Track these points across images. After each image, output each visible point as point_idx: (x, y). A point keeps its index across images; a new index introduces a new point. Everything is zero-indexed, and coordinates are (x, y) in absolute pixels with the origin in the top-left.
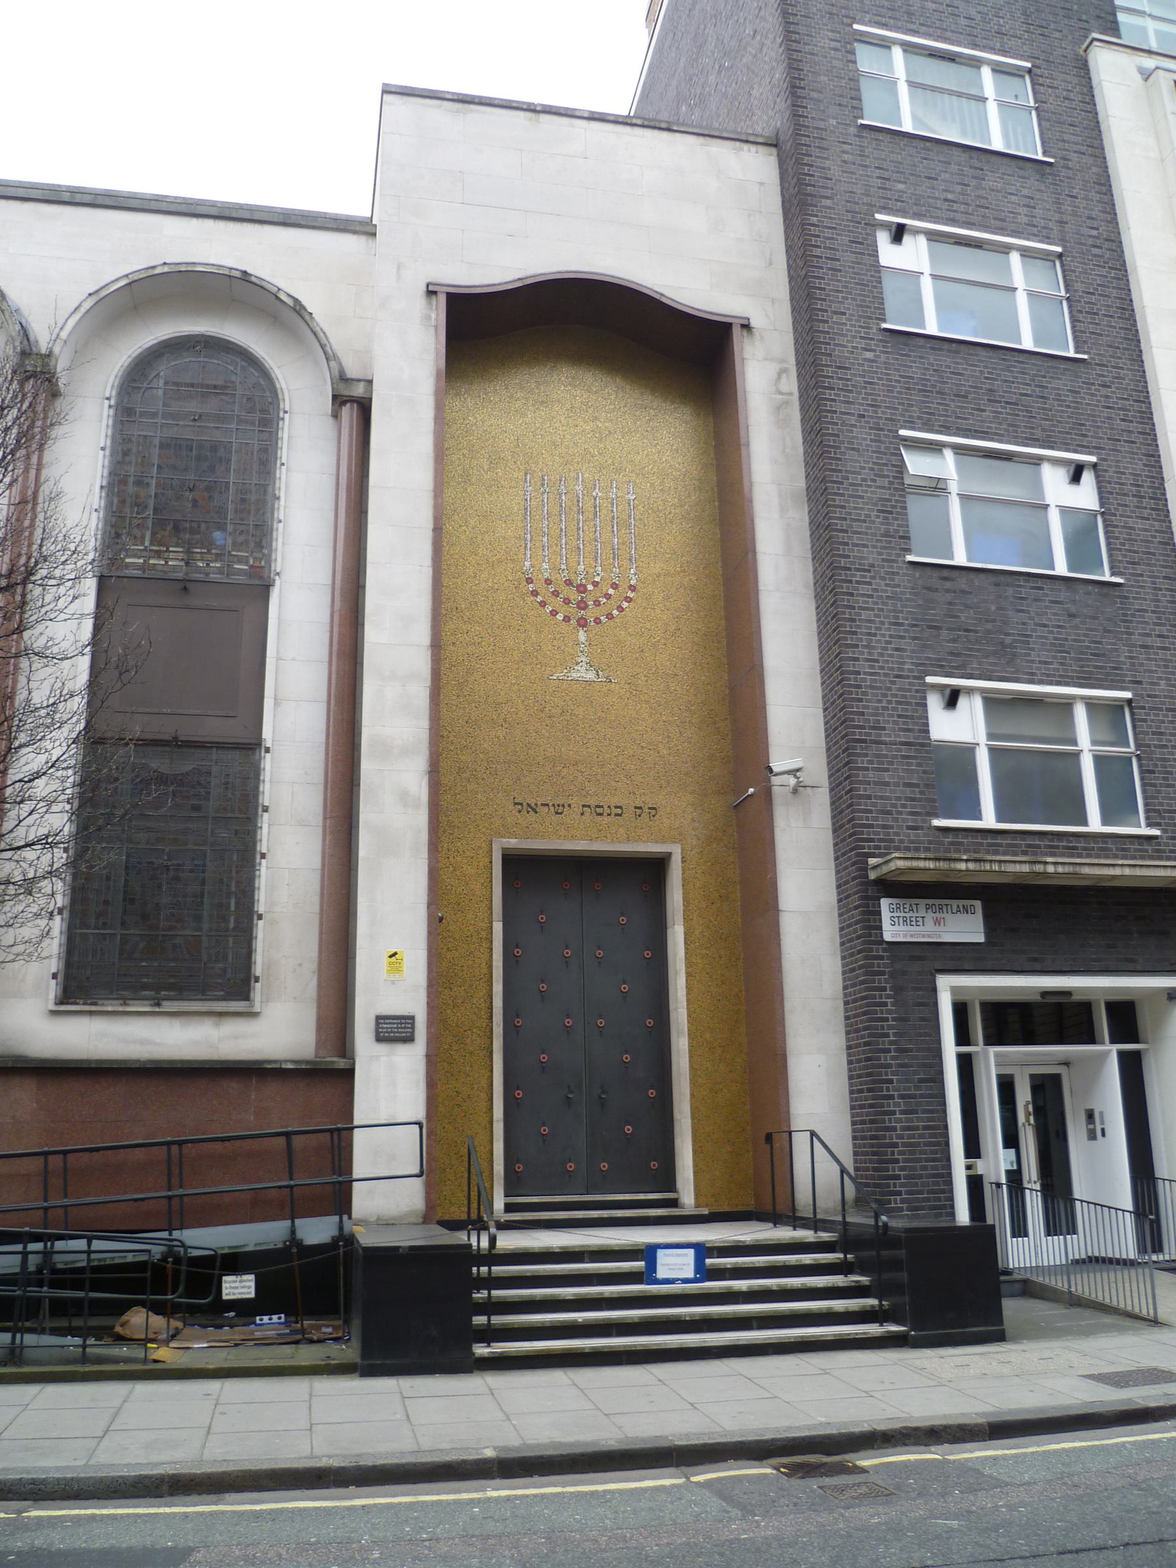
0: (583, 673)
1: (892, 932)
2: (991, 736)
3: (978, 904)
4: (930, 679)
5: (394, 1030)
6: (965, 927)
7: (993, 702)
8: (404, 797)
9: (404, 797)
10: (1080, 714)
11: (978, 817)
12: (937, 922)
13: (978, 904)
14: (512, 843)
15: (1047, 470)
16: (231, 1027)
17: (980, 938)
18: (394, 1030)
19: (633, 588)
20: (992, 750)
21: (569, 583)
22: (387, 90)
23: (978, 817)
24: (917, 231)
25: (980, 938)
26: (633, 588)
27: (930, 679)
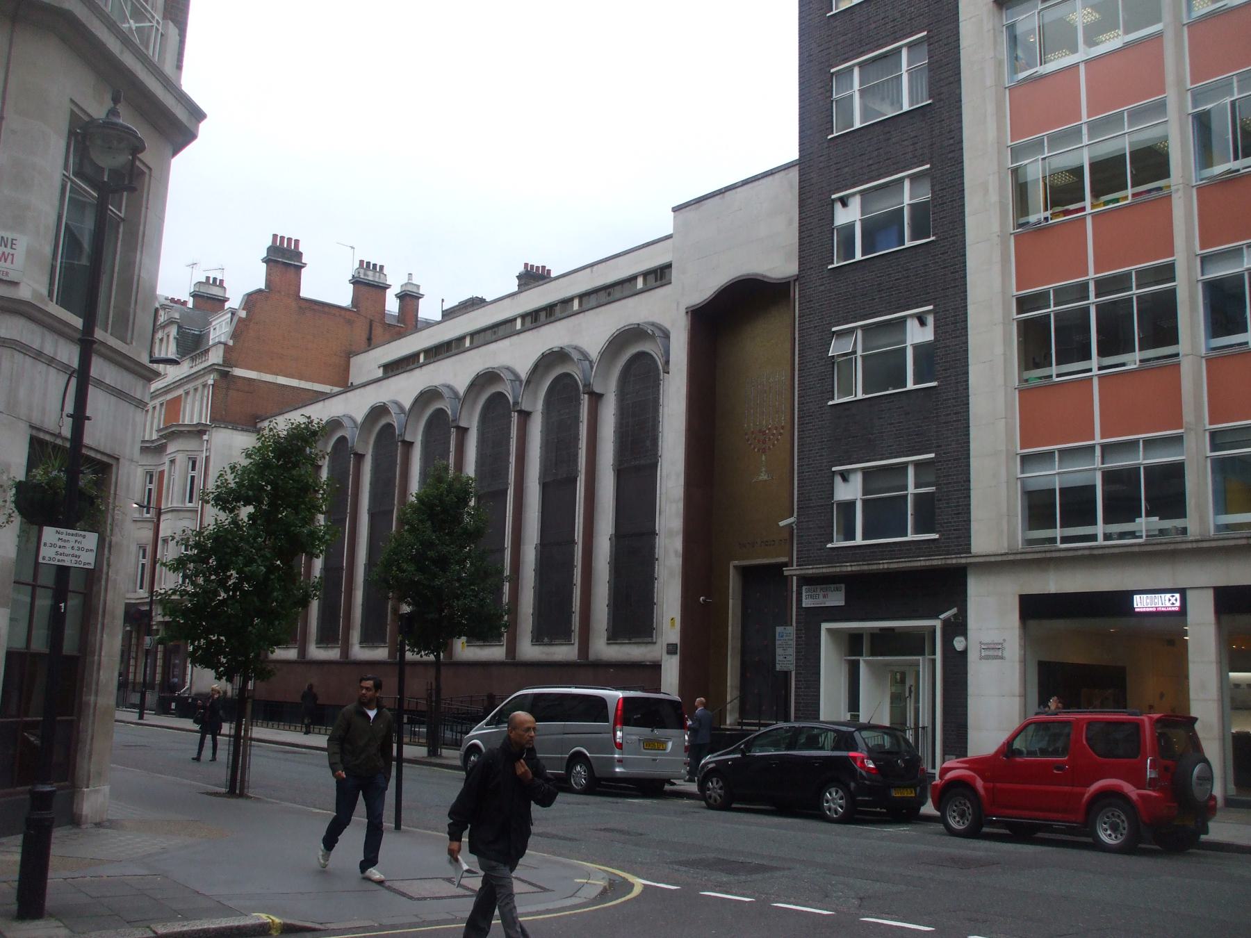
0: (763, 477)
1: (807, 603)
2: (865, 492)
3: (843, 586)
4: (834, 469)
5: (671, 649)
6: (836, 599)
7: (867, 473)
8: (676, 552)
9: (676, 552)
10: (911, 471)
11: (854, 539)
12: (824, 596)
13: (843, 586)
14: (736, 563)
15: (909, 322)
16: (650, 647)
17: (842, 603)
18: (671, 649)
19: (783, 428)
20: (865, 502)
21: (760, 431)
22: (675, 210)
23: (854, 539)
24: (853, 194)
25: (842, 603)
26: (783, 428)
27: (834, 469)
